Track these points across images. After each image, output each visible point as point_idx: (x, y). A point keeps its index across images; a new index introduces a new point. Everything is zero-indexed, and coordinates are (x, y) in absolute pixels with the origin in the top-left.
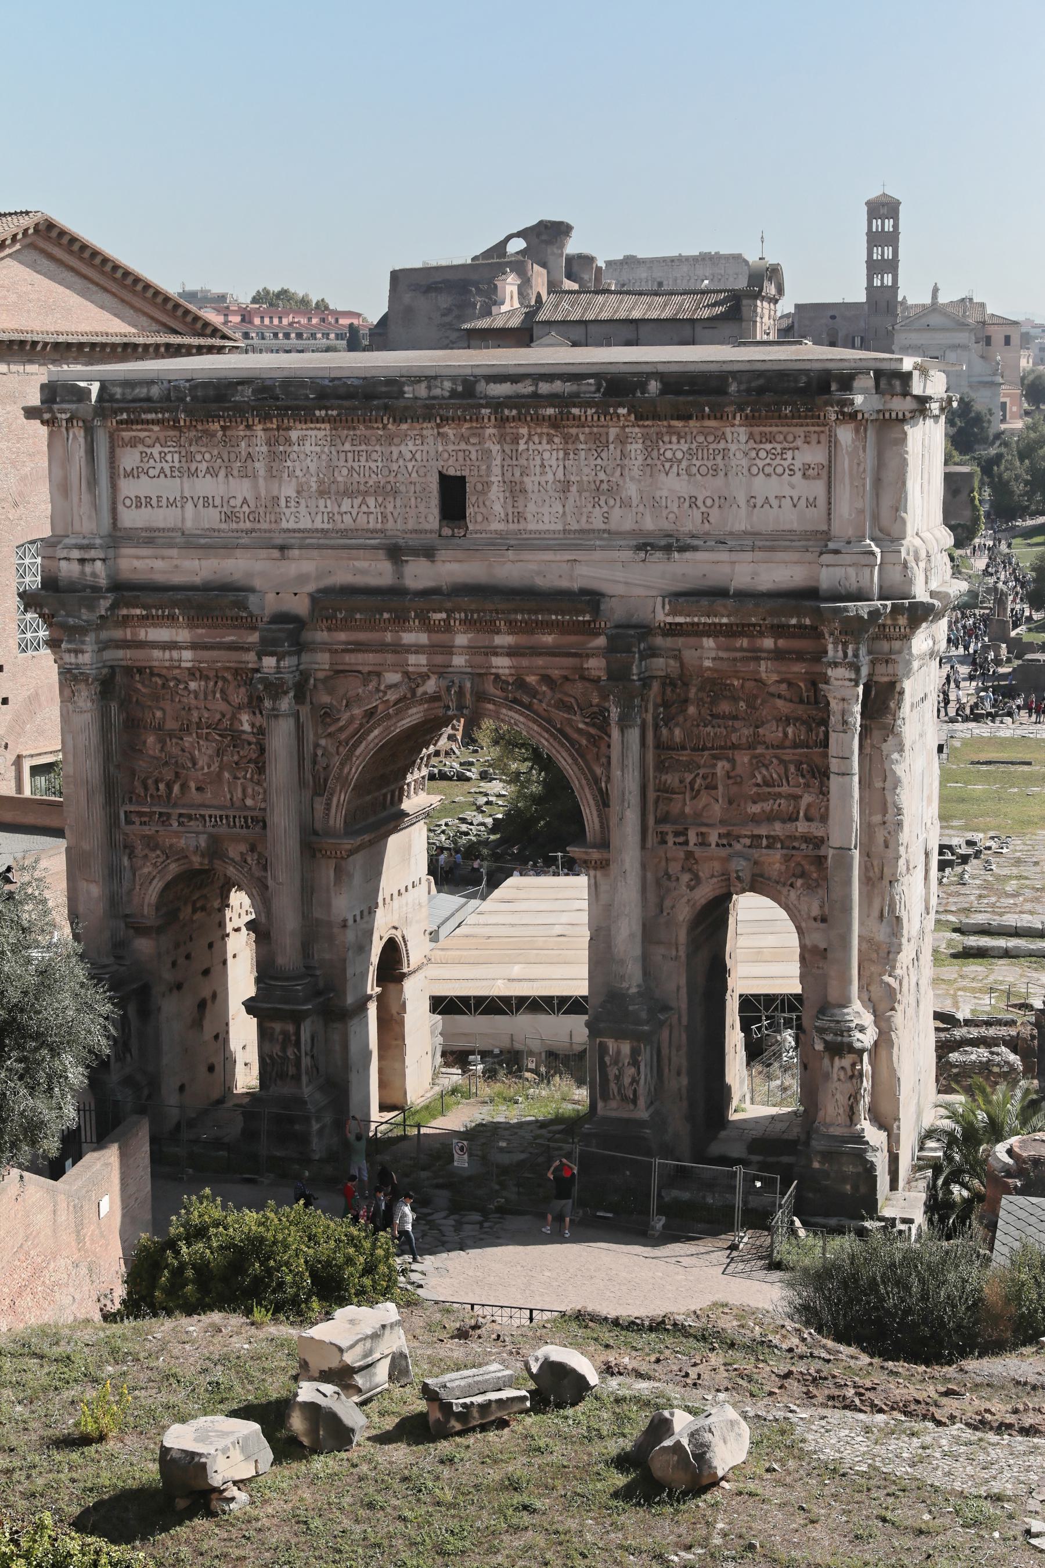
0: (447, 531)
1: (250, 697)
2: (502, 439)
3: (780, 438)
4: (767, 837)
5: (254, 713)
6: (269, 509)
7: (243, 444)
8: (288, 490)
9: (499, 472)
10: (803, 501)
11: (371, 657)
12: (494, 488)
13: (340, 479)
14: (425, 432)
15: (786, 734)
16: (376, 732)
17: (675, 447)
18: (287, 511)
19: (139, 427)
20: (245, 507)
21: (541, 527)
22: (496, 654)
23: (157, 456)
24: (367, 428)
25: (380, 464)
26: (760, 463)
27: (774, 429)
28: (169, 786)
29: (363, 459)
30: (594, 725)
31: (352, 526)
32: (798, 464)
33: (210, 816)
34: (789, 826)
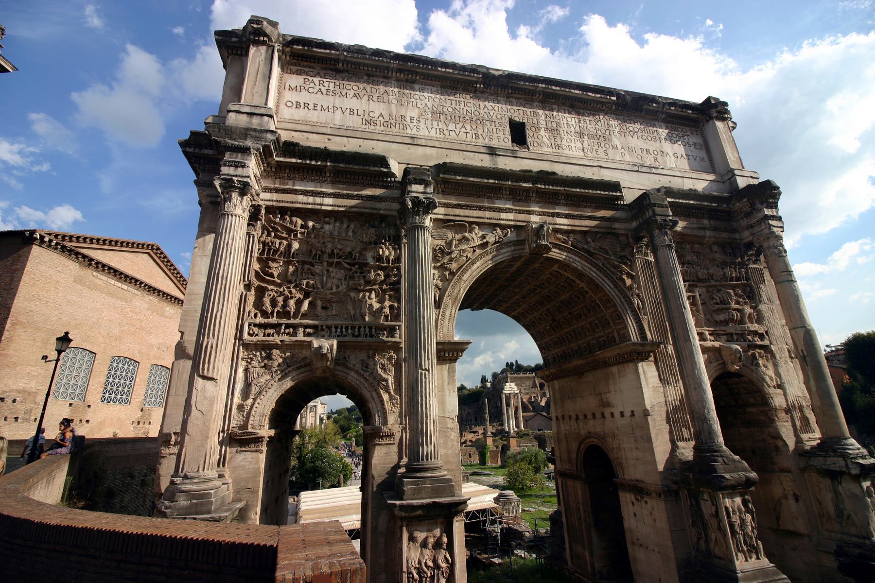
3: (680, 130)
4: (736, 334)
6: (398, 122)
8: (413, 113)
9: (543, 123)
12: (542, 132)
13: (447, 113)
16: (478, 264)
19: (306, 64)
20: (381, 118)
21: (571, 152)
22: (559, 215)
23: (317, 83)
25: (472, 109)
26: (675, 140)
27: (677, 126)
28: (299, 303)
29: (462, 105)
31: (456, 138)
32: (691, 143)
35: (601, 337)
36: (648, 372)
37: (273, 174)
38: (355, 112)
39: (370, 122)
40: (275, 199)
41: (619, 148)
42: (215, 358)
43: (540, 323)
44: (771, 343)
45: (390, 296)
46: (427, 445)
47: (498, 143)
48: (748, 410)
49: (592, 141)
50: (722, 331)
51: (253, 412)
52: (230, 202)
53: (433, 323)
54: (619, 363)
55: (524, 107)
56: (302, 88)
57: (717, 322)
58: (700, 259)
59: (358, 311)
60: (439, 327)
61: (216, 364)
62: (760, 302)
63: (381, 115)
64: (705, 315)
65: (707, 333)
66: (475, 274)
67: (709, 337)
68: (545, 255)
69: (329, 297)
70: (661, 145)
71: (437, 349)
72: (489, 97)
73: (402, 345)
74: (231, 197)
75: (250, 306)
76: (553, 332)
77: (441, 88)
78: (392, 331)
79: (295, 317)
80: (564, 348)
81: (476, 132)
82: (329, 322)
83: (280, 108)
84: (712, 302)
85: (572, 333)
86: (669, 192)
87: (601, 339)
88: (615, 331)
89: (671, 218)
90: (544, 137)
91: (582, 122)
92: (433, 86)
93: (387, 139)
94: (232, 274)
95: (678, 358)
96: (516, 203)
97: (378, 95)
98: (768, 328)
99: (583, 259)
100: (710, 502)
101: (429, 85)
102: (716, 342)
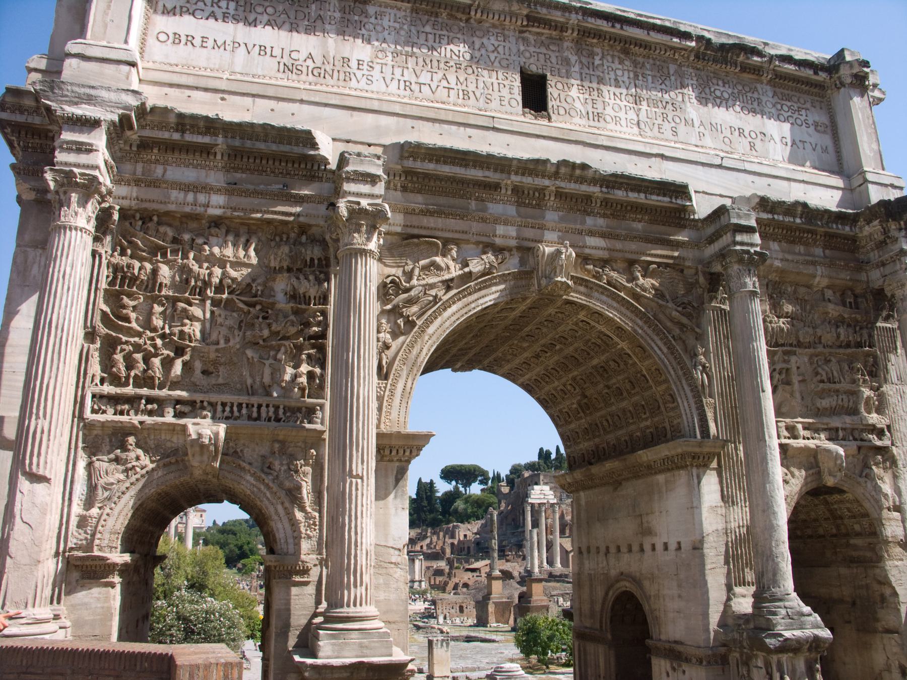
0: (529, 118)
1: (293, 259)
2: (579, 51)
3: (795, 99)
4: (844, 429)
5: (298, 278)
6: (336, 69)
7: (313, 7)
10: (819, 147)
11: (452, 223)
14: (506, 32)
15: (838, 336)
16: (454, 308)
17: (722, 89)
18: (359, 74)
20: (309, 62)
22: (591, 233)
24: (451, 16)
26: (786, 115)
28: (167, 364)
30: (683, 315)
32: (810, 122)
33: (224, 405)
34: (855, 418)
35: (647, 427)
36: (710, 485)
37: (132, 155)
38: (268, 50)
39: (291, 68)
40: (134, 195)
41: (697, 123)
42: (48, 447)
43: (563, 398)
44: (893, 444)
45: (309, 356)
46: (356, 586)
47: (499, 107)
48: (852, 541)
49: (654, 110)
50: (823, 424)
51: (100, 528)
52: (69, 208)
53: (374, 405)
54: (668, 470)
55: (548, 48)
56: (185, 9)
57: (819, 409)
58: (805, 311)
59: (258, 380)
60: (384, 409)
61: (49, 457)
62: (886, 381)
63: (310, 56)
64: (803, 398)
65: (800, 426)
66: (447, 323)
67: (802, 432)
68: (565, 297)
69: (213, 356)
70: (764, 124)
71: (377, 445)
72: (491, 30)
73: (326, 436)
74: (70, 200)
75: (95, 368)
76: (582, 414)
77: (412, 10)
78: (310, 413)
79: (161, 387)
80: (597, 440)
81: (464, 87)
82: (215, 398)
83: (147, 44)
84: (815, 380)
85: (609, 418)
86: (764, 204)
87: (648, 431)
88: (667, 420)
89: (758, 249)
90: (577, 101)
91: (640, 78)
92: (399, 9)
93: (317, 100)
94: (70, 321)
95: (747, 465)
96: (522, 210)
97: (307, 23)
98: (891, 419)
99: (623, 305)
100: (764, 670)
101: (392, 8)
102: (811, 441)
